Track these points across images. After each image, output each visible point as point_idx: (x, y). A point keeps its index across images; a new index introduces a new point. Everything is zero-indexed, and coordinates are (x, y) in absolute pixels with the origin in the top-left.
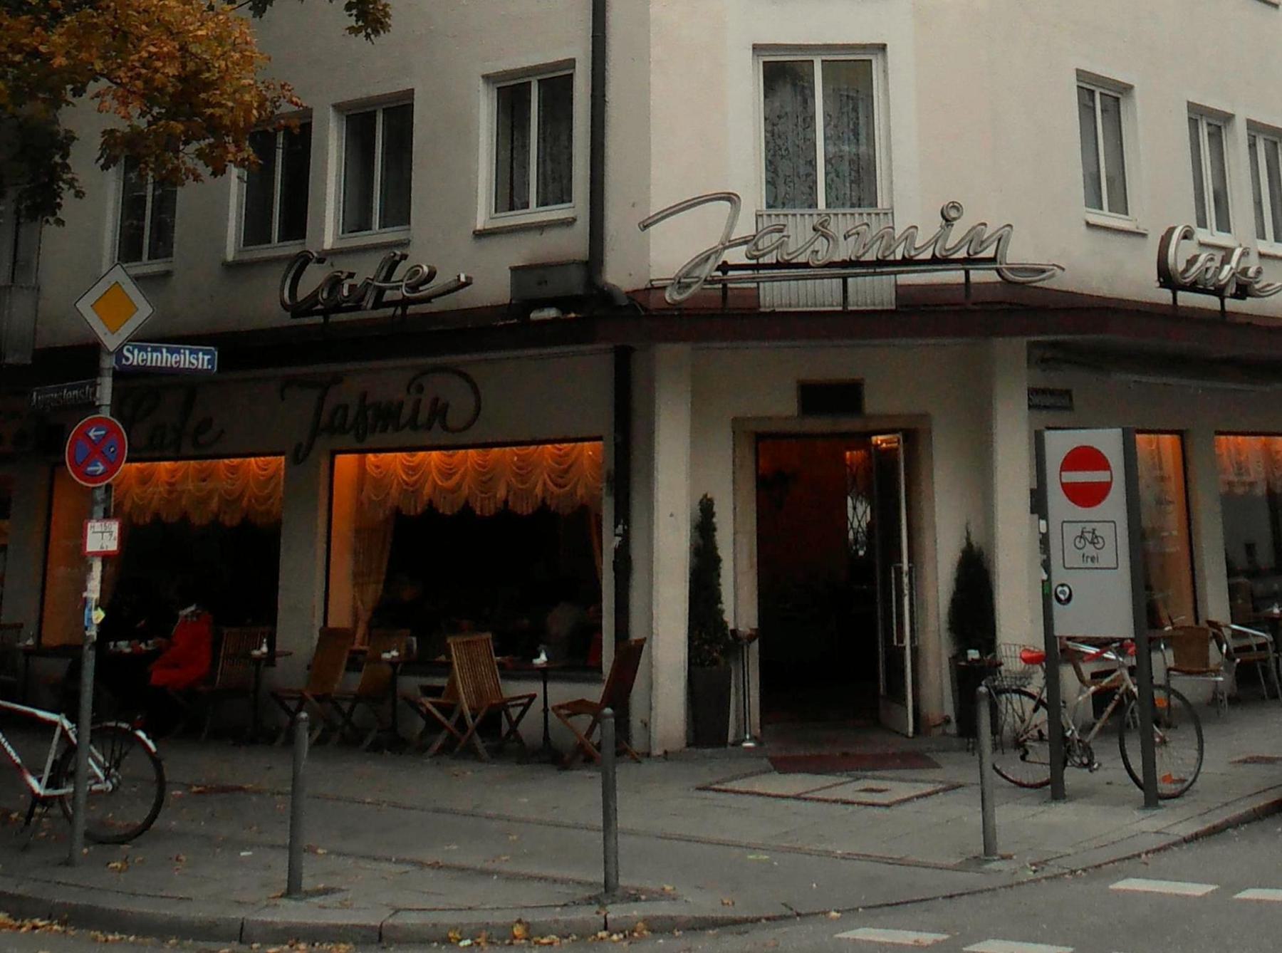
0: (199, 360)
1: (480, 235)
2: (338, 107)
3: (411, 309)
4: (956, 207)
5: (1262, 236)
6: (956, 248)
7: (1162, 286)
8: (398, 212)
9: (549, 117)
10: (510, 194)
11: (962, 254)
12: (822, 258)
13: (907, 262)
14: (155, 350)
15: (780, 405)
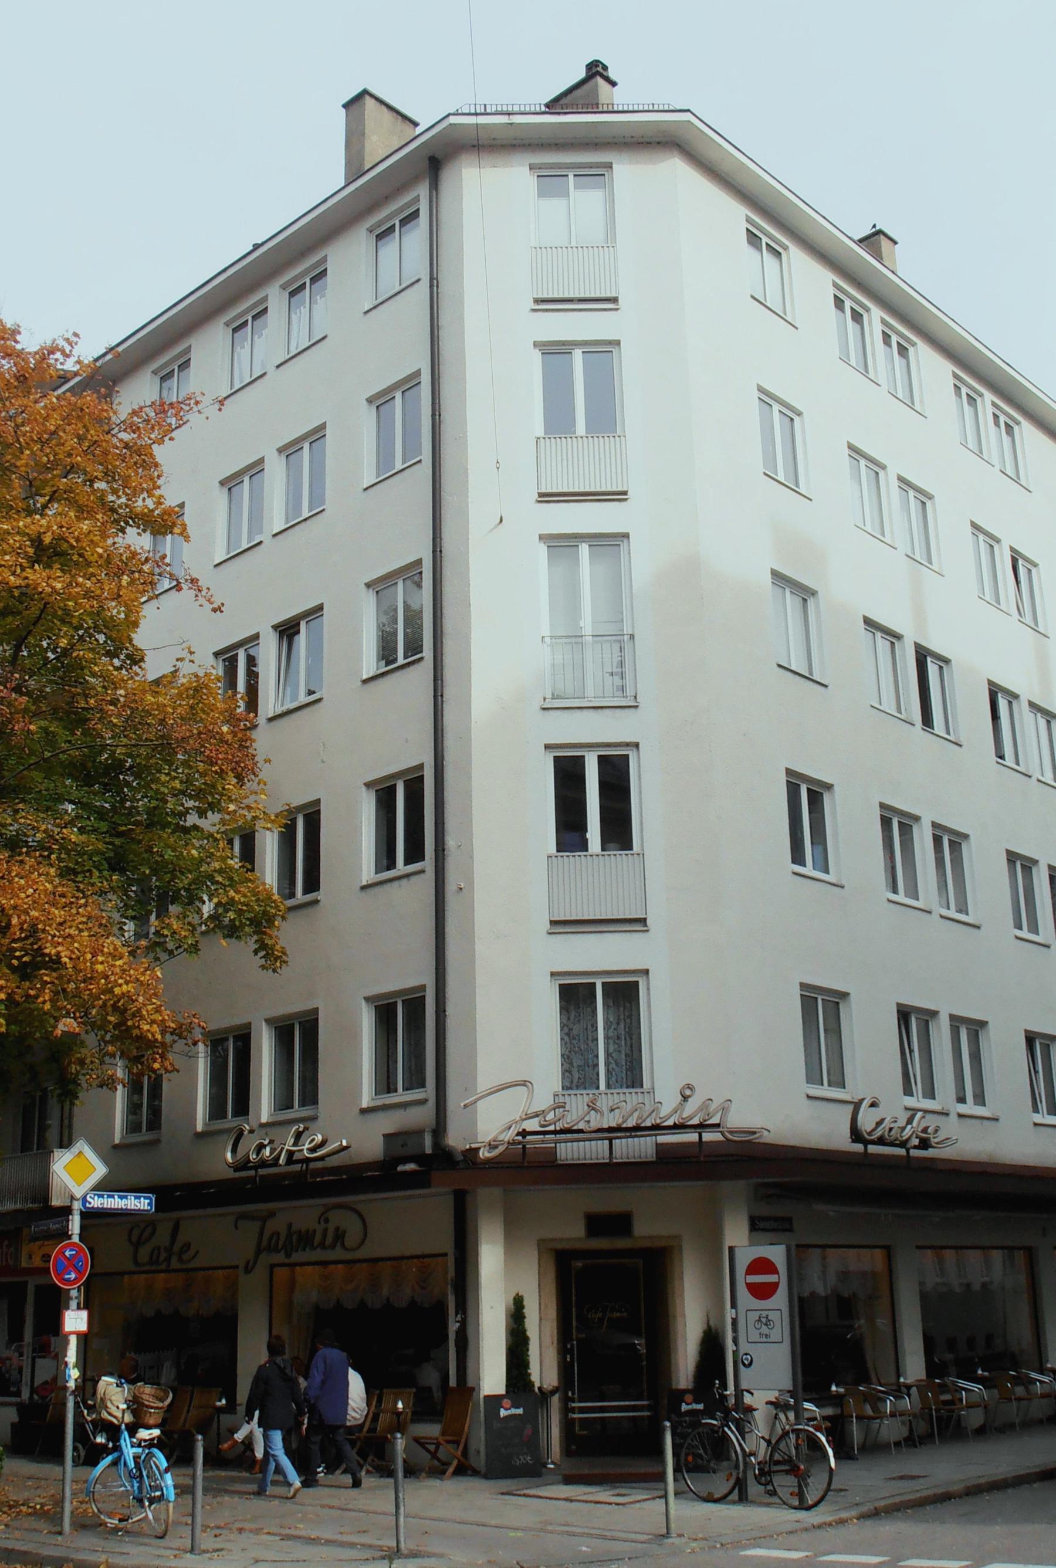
0: (140, 1203)
1: (364, 1111)
2: (268, 1021)
3: (312, 1165)
4: (689, 1087)
5: (962, 1100)
6: (691, 1118)
7: (853, 1141)
8: (310, 1097)
9: (413, 1027)
10: (385, 1083)
11: (695, 1121)
12: (594, 1125)
13: (656, 1127)
14: (109, 1196)
15: (572, 1232)
